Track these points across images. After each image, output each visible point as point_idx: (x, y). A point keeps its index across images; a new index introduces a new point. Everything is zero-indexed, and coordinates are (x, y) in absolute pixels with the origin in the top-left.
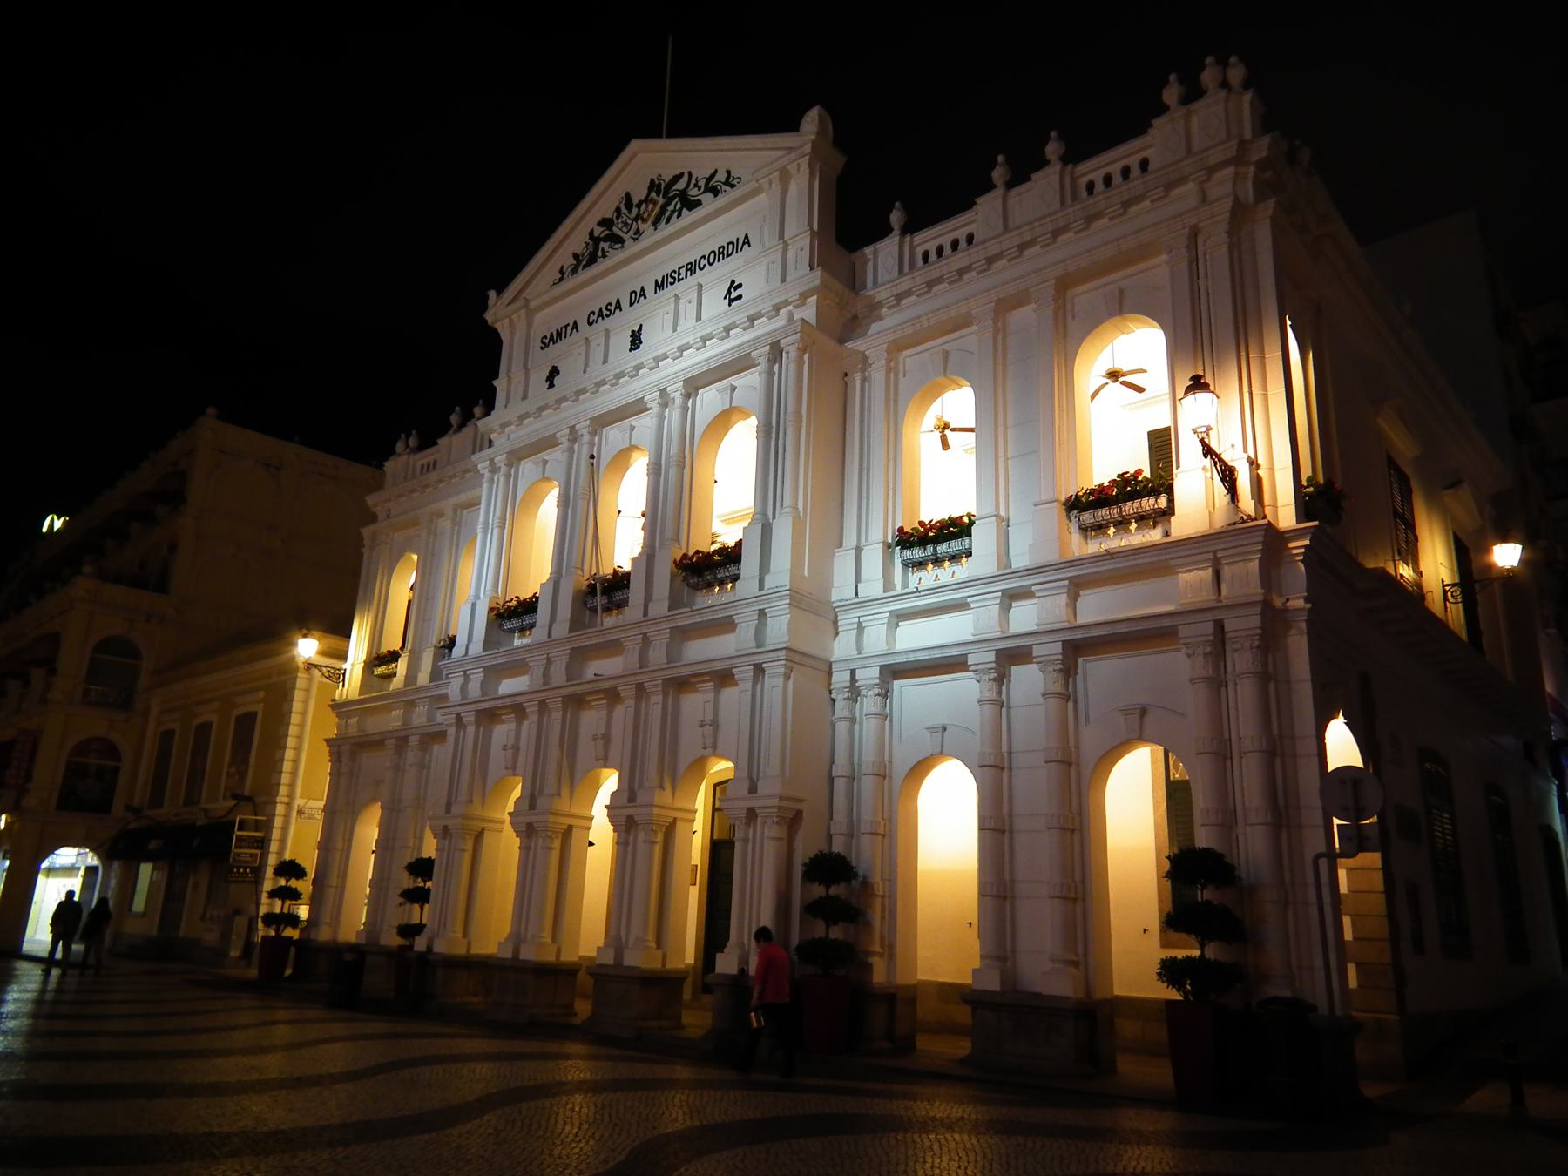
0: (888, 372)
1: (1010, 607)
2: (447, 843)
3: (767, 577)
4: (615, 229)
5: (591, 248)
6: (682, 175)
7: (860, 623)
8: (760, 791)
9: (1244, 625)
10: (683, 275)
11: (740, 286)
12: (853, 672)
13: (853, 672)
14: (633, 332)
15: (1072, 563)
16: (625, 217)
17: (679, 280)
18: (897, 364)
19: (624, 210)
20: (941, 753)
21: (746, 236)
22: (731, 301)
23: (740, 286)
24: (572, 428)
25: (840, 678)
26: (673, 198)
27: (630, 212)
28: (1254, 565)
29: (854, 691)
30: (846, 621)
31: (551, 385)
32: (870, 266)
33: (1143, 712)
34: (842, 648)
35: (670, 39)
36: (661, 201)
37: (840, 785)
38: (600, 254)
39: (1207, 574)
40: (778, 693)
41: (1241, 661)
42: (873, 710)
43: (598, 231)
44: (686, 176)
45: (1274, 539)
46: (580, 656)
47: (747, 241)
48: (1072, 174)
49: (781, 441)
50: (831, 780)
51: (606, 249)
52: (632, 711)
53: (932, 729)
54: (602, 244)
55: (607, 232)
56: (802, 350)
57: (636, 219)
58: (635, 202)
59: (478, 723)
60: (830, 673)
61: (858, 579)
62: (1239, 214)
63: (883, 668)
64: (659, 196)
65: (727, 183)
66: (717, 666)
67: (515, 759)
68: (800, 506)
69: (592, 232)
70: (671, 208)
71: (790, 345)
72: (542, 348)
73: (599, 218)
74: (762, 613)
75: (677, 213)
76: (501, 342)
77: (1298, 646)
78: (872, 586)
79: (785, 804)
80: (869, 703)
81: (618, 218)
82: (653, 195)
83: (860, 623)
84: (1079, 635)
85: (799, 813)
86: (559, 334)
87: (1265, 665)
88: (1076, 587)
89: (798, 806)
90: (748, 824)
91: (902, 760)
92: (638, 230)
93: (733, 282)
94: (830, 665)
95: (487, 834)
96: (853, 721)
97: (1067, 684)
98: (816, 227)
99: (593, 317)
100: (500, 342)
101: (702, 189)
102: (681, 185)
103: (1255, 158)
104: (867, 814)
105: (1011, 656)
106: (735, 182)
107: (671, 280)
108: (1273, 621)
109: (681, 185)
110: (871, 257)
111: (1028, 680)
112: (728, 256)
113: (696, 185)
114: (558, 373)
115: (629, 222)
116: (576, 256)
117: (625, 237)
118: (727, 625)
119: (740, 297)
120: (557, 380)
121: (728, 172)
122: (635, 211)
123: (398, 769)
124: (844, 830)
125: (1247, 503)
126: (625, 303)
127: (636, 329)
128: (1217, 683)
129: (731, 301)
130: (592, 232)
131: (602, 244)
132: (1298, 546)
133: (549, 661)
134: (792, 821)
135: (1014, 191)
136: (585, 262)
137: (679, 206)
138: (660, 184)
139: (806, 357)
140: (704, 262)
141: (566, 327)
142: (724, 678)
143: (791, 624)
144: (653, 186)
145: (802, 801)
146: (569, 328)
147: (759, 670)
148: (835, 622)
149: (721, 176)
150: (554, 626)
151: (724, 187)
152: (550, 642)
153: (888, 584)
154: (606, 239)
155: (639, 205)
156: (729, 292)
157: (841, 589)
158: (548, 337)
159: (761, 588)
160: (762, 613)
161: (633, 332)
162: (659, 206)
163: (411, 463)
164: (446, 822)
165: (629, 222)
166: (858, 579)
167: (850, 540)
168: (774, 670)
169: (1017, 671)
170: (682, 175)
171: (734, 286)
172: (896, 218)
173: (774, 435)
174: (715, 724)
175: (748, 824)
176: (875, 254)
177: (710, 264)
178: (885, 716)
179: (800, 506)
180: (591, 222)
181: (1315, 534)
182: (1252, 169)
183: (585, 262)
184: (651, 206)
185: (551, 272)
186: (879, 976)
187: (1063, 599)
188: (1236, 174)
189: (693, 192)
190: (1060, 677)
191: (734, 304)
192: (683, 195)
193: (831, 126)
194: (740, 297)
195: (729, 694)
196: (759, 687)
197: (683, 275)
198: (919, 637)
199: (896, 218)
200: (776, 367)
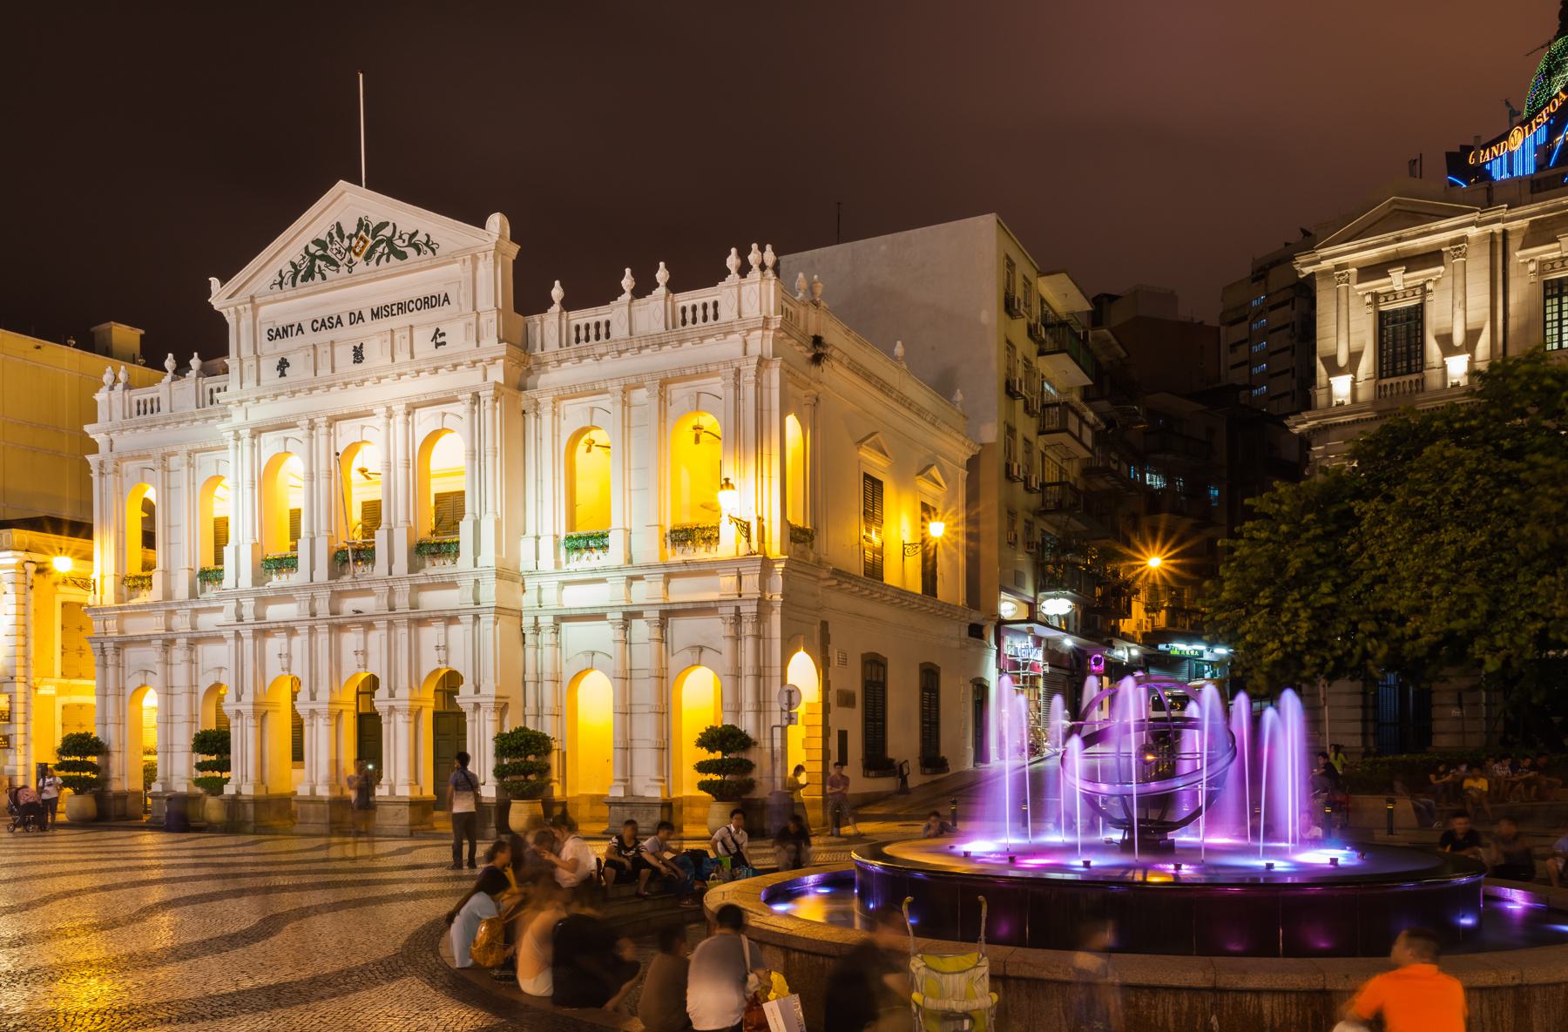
0: (554, 414)
1: (631, 584)
2: (239, 721)
3: (479, 558)
4: (328, 251)
5: (307, 263)
6: (387, 224)
7: (539, 587)
8: (482, 692)
9: (749, 609)
10: (395, 312)
11: (443, 334)
12: (536, 618)
13: (536, 618)
14: (355, 347)
15: (666, 566)
16: (338, 246)
17: (393, 315)
18: (559, 409)
19: (336, 238)
20: (591, 668)
21: (446, 295)
22: (437, 345)
23: (443, 334)
24: (311, 421)
25: (528, 621)
26: (381, 241)
27: (342, 242)
28: (757, 577)
29: (537, 629)
30: (530, 584)
31: (283, 375)
32: (539, 329)
33: (701, 649)
34: (528, 600)
35: (361, 76)
36: (371, 242)
37: (530, 687)
38: (317, 269)
39: (735, 579)
40: (490, 633)
41: (748, 628)
42: (549, 642)
43: (313, 249)
44: (391, 226)
45: (766, 564)
46: (337, 596)
47: (446, 299)
48: (672, 300)
49: (482, 463)
50: (524, 683)
51: (323, 268)
52: (385, 638)
53: (585, 653)
54: (318, 262)
55: (321, 252)
56: (496, 400)
57: (350, 249)
58: (347, 233)
59: (255, 638)
60: (521, 617)
61: (537, 558)
62: (762, 362)
63: (556, 617)
64: (367, 235)
65: (427, 244)
66: (448, 614)
67: (289, 662)
68: (499, 511)
69: (307, 248)
70: (380, 249)
71: (487, 395)
72: (270, 340)
73: (313, 237)
74: (477, 581)
75: (385, 257)
76: (227, 325)
77: (776, 619)
78: (547, 562)
79: (499, 700)
80: (547, 637)
81: (331, 242)
82: (362, 233)
83: (539, 587)
84: (668, 607)
85: (507, 704)
86: (285, 331)
87: (759, 630)
88: (668, 577)
89: (505, 700)
90: (474, 711)
91: (568, 673)
92: (351, 261)
93: (438, 330)
94: (521, 612)
95: (270, 715)
96: (537, 646)
97: (662, 633)
98: (500, 306)
99: (316, 326)
100: (227, 325)
101: (406, 243)
102: (387, 232)
103: (773, 327)
104: (548, 702)
105: (630, 616)
106: (434, 246)
107: (384, 313)
108: (763, 605)
109: (387, 232)
110: (538, 322)
111: (642, 630)
112: (432, 307)
113: (400, 237)
114: (288, 365)
115: (343, 251)
116: (293, 265)
117: (340, 263)
118: (452, 585)
119: (444, 343)
120: (287, 370)
121: (428, 236)
122: (346, 243)
123: (167, 663)
124: (534, 713)
125: (755, 546)
126: (345, 319)
127: (358, 346)
128: (737, 638)
129: (437, 345)
130: (307, 248)
131: (318, 262)
132: (779, 567)
133: (313, 598)
134: (502, 709)
135: (637, 302)
136: (302, 273)
137: (386, 251)
138: (367, 225)
139: (498, 405)
140: (412, 306)
141: (292, 326)
142: (451, 619)
143: (497, 590)
144: (361, 224)
145: (507, 697)
146: (295, 329)
147: (477, 617)
148: (523, 584)
149: (421, 238)
150: (314, 573)
151: (425, 248)
152: (311, 585)
153: (557, 565)
154: (322, 258)
155: (350, 237)
156: (435, 337)
157: (527, 564)
158: (275, 330)
159: (475, 566)
160: (477, 581)
161: (355, 347)
162: (368, 247)
163: (127, 397)
164: (238, 708)
165: (343, 251)
166: (537, 558)
167: (531, 531)
168: (487, 620)
169: (634, 622)
170: (387, 224)
171: (438, 333)
172: (557, 292)
173: (477, 457)
174: (446, 648)
175: (474, 711)
176: (542, 321)
177: (419, 309)
178: (557, 645)
179: (499, 511)
180: (306, 239)
181: (787, 561)
182: (772, 333)
183: (302, 273)
184: (361, 243)
185: (271, 275)
186: (557, 792)
187: (661, 585)
188: (763, 335)
189: (398, 242)
190: (658, 630)
191: (439, 347)
192: (390, 241)
193: (508, 228)
194: (444, 343)
195: (455, 630)
196: (477, 627)
197: (395, 312)
198: (579, 598)
199: (557, 292)
200: (476, 408)
